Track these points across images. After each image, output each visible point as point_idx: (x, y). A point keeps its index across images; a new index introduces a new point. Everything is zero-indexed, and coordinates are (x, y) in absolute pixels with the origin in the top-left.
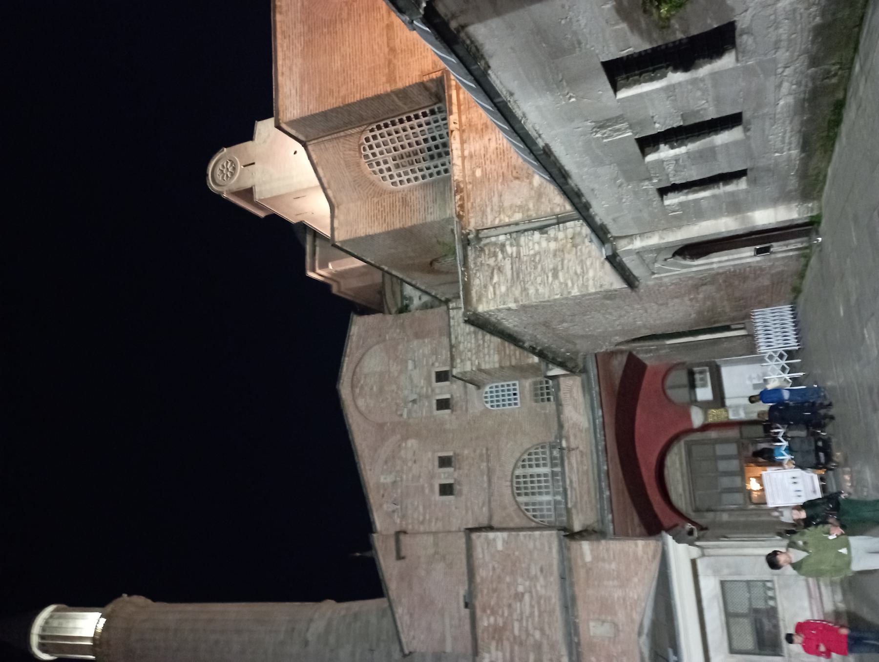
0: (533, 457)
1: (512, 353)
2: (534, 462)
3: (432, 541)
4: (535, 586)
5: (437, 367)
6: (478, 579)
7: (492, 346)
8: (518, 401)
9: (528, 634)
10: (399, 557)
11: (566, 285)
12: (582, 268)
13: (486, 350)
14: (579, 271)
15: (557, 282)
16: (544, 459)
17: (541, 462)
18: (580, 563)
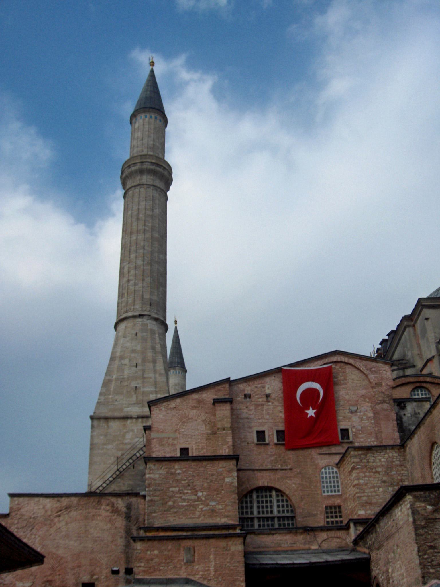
0: (285, 503)
1: (366, 494)
2: (281, 504)
3: (226, 426)
4: (202, 504)
5: (352, 430)
6: (205, 463)
7: (370, 479)
8: (326, 494)
9: (171, 497)
10: (216, 402)
11: (425, 554)
12: (435, 565)
13: (367, 474)
14: (434, 563)
15: (427, 548)
16: (283, 511)
17: (281, 509)
18: (230, 543)
